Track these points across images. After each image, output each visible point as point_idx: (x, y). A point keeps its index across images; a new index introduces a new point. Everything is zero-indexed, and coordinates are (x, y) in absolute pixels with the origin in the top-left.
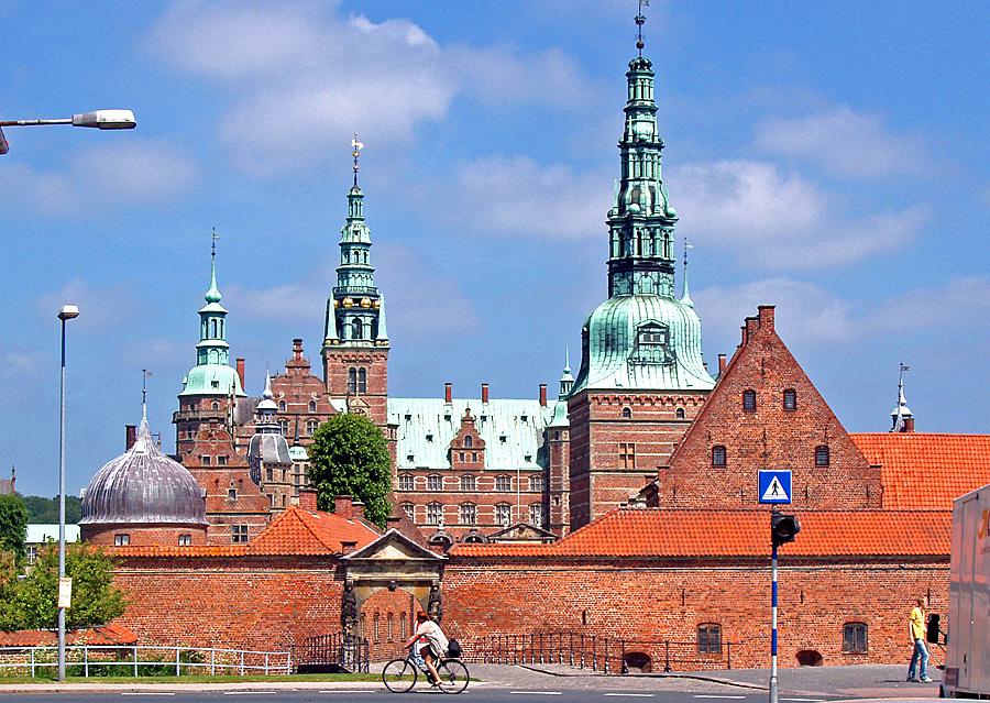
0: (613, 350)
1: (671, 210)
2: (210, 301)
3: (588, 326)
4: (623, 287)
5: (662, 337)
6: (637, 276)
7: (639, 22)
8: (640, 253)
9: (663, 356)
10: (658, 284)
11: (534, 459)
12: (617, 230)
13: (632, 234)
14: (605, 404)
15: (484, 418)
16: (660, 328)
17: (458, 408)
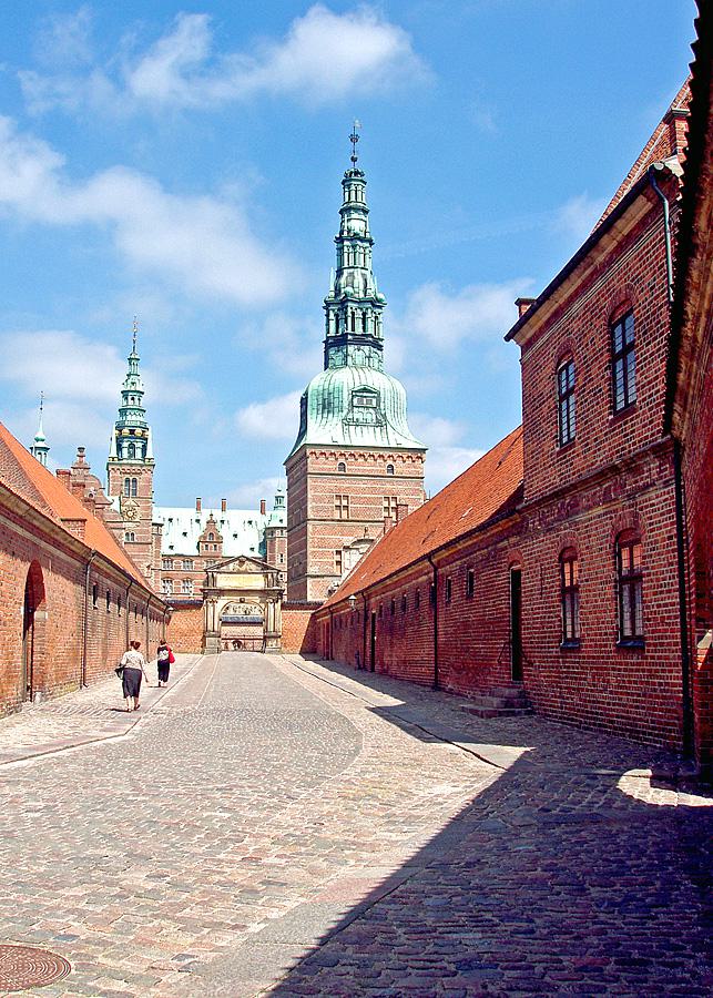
0: (328, 412)
1: (380, 296)
2: (37, 440)
3: (306, 394)
4: (337, 358)
5: (374, 400)
6: (351, 349)
7: (354, 139)
8: (353, 329)
9: (374, 418)
10: (369, 357)
11: (257, 549)
12: (333, 310)
13: (346, 313)
14: (322, 458)
15: (222, 522)
16: (370, 392)
17: (204, 518)
